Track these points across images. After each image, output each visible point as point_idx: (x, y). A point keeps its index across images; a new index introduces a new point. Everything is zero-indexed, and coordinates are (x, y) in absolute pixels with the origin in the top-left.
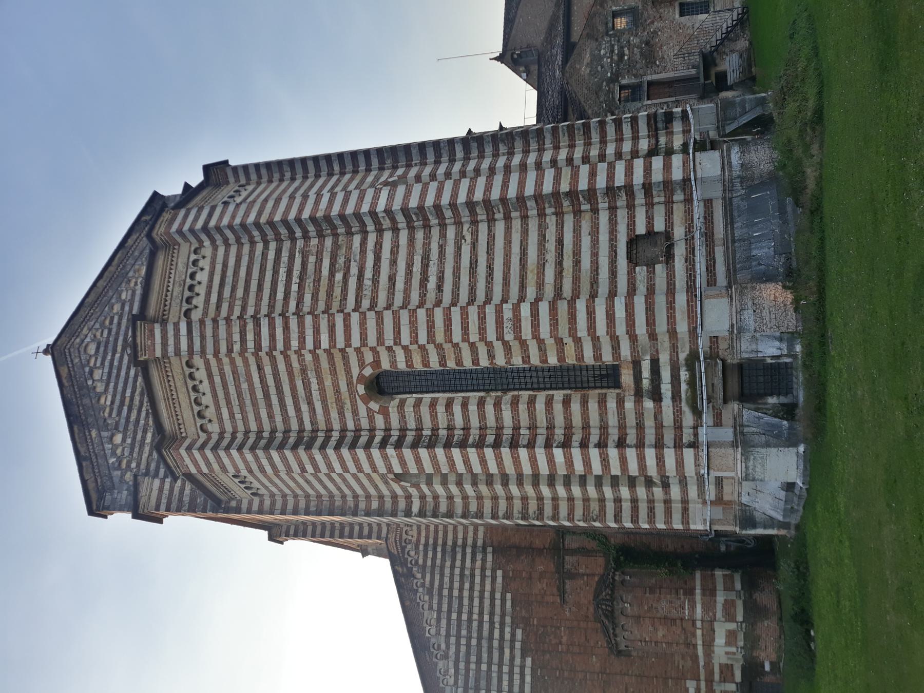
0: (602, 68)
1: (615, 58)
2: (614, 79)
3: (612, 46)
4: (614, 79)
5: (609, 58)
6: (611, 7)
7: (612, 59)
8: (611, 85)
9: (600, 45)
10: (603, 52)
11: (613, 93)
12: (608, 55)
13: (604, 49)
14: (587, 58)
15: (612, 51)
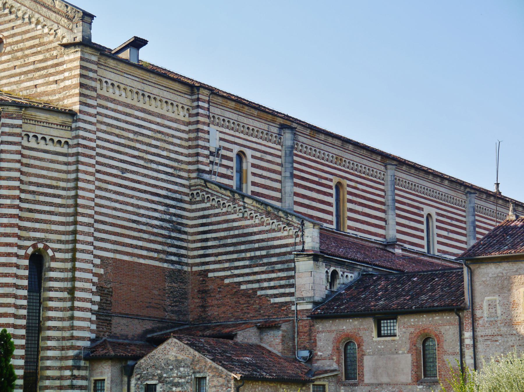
0: (171, 369)
1: (176, 380)
2: (161, 380)
3: (185, 378)
4: (161, 380)
5: (177, 374)
6: (209, 376)
7: (175, 377)
8: (157, 378)
9: (187, 367)
10: (182, 369)
11: (152, 379)
12: (179, 374)
13: (184, 371)
14: (180, 357)
15: (181, 378)
